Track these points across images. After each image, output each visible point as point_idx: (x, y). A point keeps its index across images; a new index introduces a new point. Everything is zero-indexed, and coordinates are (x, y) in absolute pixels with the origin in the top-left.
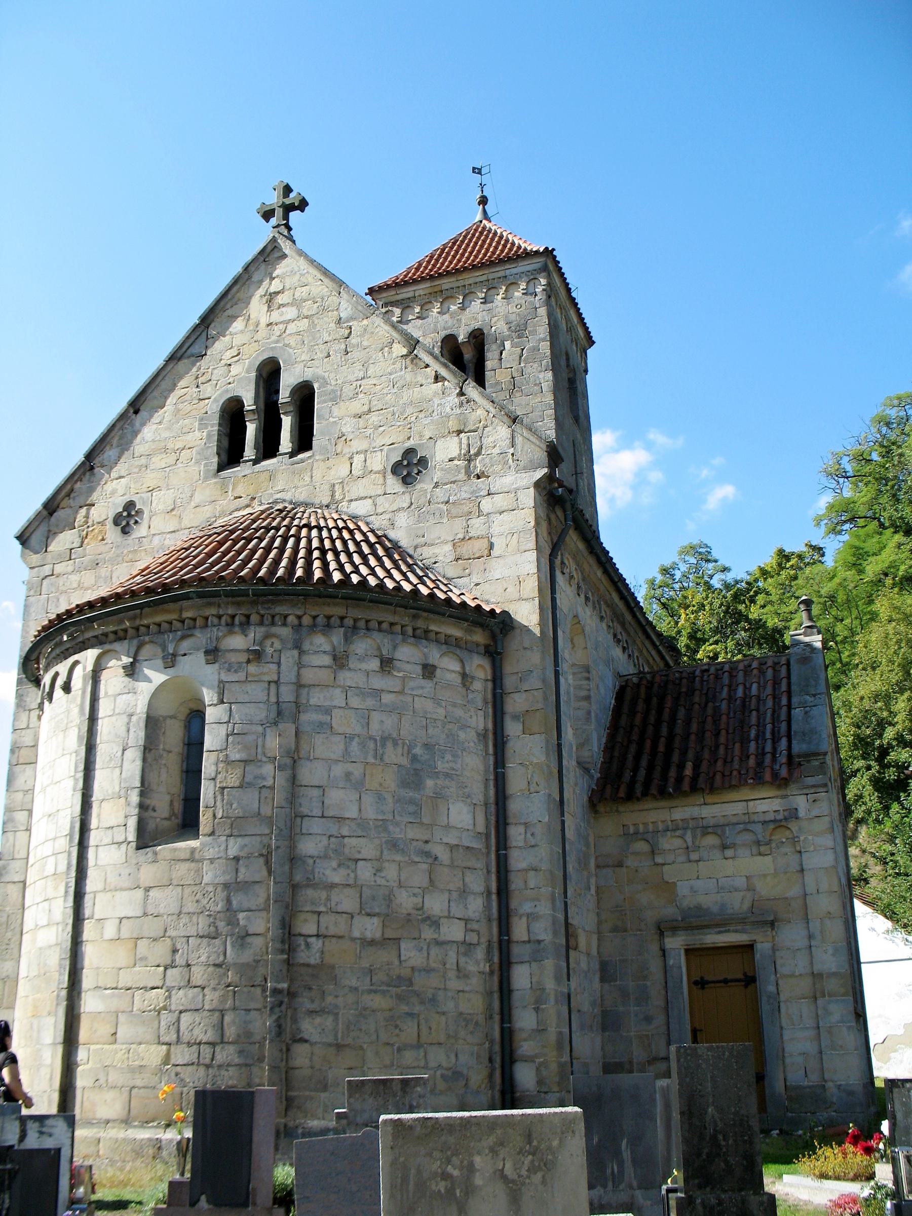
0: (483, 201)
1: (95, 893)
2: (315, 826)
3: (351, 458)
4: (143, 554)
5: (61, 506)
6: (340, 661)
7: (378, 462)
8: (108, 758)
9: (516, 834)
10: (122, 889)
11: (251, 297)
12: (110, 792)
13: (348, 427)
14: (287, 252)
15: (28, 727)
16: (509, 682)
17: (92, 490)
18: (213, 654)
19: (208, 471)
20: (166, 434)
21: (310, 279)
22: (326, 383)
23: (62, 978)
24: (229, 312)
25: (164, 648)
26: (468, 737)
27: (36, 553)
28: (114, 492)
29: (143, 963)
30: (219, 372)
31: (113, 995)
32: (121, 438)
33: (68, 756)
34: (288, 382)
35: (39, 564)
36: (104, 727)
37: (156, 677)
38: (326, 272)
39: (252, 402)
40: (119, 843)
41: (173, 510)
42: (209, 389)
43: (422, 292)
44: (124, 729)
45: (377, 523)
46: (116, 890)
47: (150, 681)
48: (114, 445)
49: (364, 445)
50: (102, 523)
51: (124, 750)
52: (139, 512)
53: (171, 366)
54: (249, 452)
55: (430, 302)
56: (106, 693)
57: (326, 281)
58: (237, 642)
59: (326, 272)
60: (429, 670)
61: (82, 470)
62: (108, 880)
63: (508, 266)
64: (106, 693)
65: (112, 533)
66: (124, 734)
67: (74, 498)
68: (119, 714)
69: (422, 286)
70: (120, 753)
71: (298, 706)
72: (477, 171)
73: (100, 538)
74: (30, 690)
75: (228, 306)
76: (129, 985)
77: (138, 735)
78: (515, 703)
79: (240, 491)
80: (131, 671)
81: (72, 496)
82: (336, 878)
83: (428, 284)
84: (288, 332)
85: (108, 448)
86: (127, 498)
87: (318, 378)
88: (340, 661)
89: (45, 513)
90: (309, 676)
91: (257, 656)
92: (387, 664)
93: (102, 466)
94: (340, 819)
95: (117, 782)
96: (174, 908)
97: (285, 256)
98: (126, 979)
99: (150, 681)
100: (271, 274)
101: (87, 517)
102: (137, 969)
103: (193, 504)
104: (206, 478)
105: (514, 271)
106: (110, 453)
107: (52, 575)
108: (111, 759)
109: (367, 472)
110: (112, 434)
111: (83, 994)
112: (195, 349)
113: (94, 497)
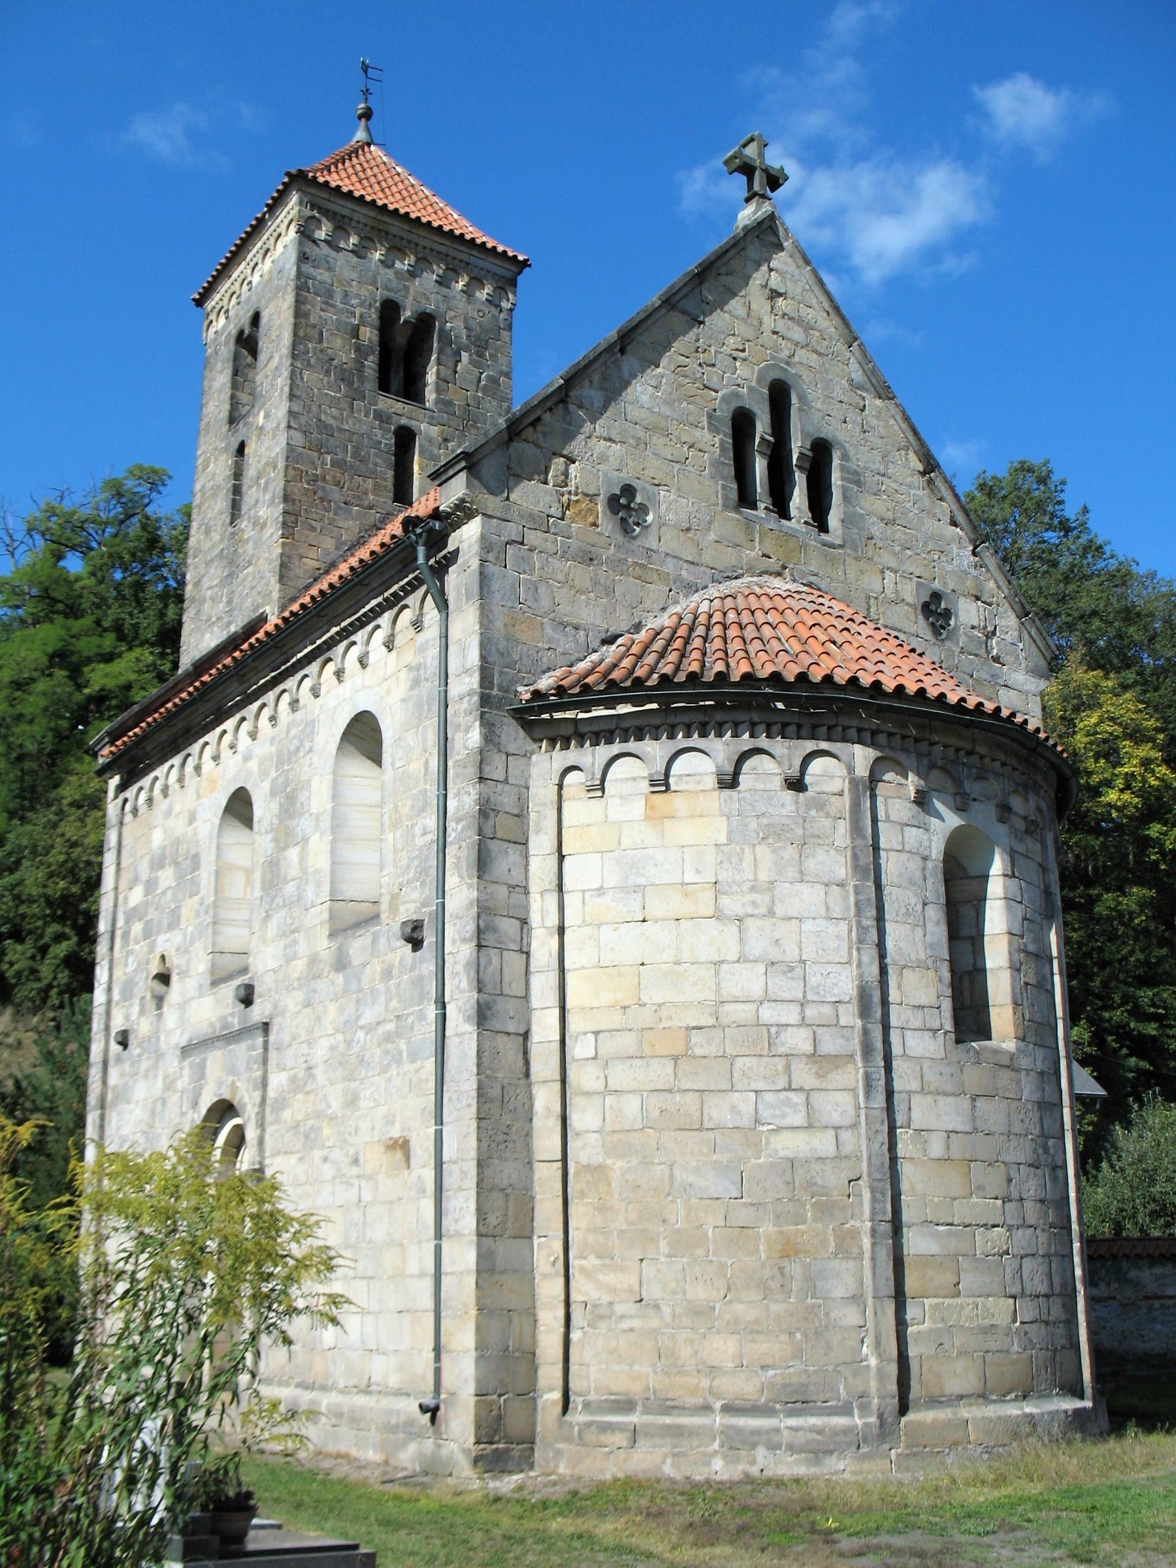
1: (909, 1093)
3: (882, 572)
4: (655, 576)
5: (524, 435)
8: (903, 910)
10: (946, 1094)
11: (749, 277)
12: (913, 957)
13: (877, 529)
14: (785, 244)
15: (506, 781)
17: (570, 436)
19: (726, 498)
20: (666, 411)
21: (814, 301)
22: (845, 457)
23: (878, 1207)
24: (724, 280)
25: (958, 782)
27: (492, 493)
28: (603, 458)
29: (981, 1194)
30: (723, 362)
31: (949, 1233)
32: (604, 379)
33: (820, 890)
35: (499, 515)
36: (891, 865)
37: (953, 821)
38: (837, 309)
39: (769, 431)
40: (935, 1031)
41: (688, 529)
42: (715, 379)
43: (363, 220)
44: (919, 874)
46: (938, 1094)
47: (942, 820)
48: (595, 383)
49: (893, 564)
50: (592, 497)
51: (925, 904)
52: (643, 509)
53: (663, 311)
55: (372, 240)
56: (887, 816)
57: (836, 320)
58: (1016, 803)
59: (837, 309)
61: (555, 399)
62: (926, 1078)
63: (475, 253)
64: (887, 816)
65: (607, 524)
66: (920, 882)
67: (545, 435)
68: (910, 852)
69: (365, 211)
70: (919, 907)
72: (365, 68)
73: (591, 519)
74: (505, 720)
75: (723, 271)
76: (967, 1221)
77: (935, 888)
79: (769, 547)
80: (921, 800)
81: (539, 428)
83: (373, 214)
84: (796, 359)
85: (586, 383)
86: (626, 476)
87: (842, 447)
89: (506, 436)
93: (580, 407)
95: (920, 946)
96: (1003, 1128)
97: (780, 247)
98: (961, 1212)
99: (942, 820)
100: (768, 260)
101: (566, 474)
102: (974, 1199)
103: (712, 536)
105: (481, 264)
106: (590, 393)
107: (522, 543)
108: (908, 914)
109: (898, 601)
110: (594, 367)
111: (905, 1230)
112: (690, 305)
113: (575, 447)
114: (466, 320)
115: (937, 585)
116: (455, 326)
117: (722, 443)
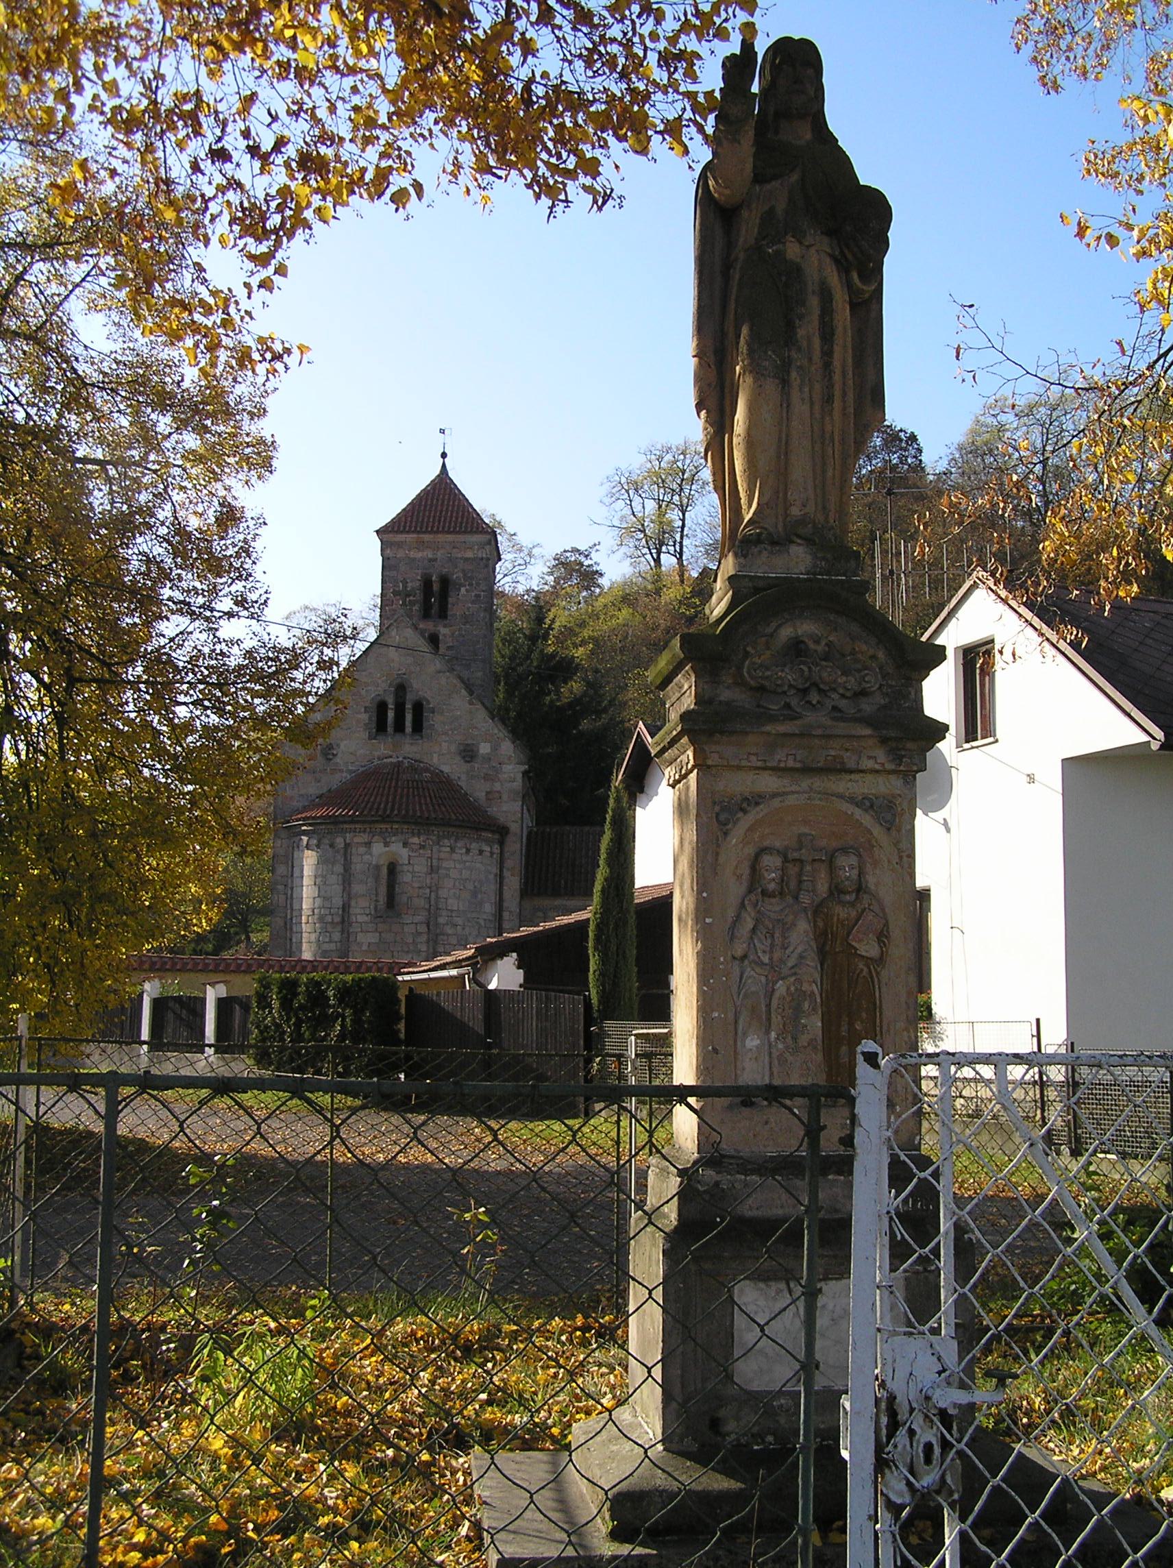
0: (444, 455)
2: (444, 913)
6: (453, 850)
7: (453, 748)
9: (506, 915)
16: (506, 855)
18: (405, 844)
22: (428, 702)
26: (491, 877)
34: (410, 698)
36: (358, 867)
45: (452, 777)
54: (390, 729)
58: (415, 840)
60: (481, 852)
65: (320, 758)
71: (439, 868)
72: (442, 431)
78: (509, 863)
82: (450, 932)
88: (453, 850)
90: (442, 855)
91: (422, 847)
92: (468, 851)
94: (452, 911)
104: (370, 738)
114: (463, 571)
115: (469, 742)
116: (456, 575)
117: (370, 719)
